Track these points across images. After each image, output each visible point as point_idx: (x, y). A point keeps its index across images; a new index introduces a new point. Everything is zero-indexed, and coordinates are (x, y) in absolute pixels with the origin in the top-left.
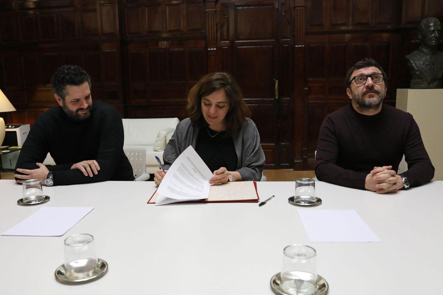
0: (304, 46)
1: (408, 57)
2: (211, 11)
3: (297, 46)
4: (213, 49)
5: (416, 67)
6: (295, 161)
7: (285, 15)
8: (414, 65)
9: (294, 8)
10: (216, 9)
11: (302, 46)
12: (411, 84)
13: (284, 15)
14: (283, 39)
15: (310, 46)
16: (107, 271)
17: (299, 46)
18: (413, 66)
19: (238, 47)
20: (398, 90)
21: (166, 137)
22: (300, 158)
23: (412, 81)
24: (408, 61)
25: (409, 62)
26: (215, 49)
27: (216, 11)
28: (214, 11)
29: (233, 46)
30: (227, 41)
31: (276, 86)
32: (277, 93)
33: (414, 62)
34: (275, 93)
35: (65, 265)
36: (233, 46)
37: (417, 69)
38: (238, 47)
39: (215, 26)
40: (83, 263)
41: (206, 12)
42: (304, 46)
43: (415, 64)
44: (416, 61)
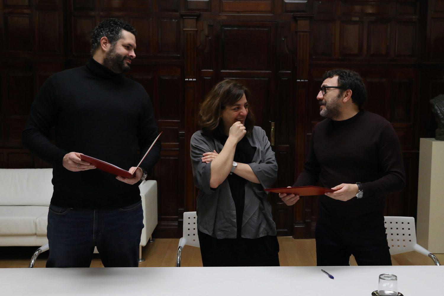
0: (307, 81)
1: (432, 101)
3: (299, 81)
4: (191, 80)
5: (441, 115)
6: (296, 226)
8: (439, 112)
9: (296, 32)
10: (196, 28)
11: (305, 81)
12: (436, 134)
18: (437, 114)
22: (301, 222)
23: (437, 130)
25: (434, 108)
27: (197, 31)
30: (210, 69)
31: (272, 129)
33: (439, 109)
34: (271, 138)
37: (442, 117)
41: (184, 31)
42: (307, 81)
43: (441, 112)
44: (441, 107)
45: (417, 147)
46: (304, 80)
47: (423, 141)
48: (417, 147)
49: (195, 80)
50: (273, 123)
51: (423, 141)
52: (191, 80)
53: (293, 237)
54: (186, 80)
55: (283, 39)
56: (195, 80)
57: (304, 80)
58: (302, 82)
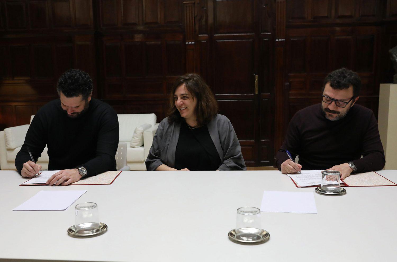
0: (284, 40)
1: (391, 51)
2: (190, 3)
3: (278, 40)
4: (191, 43)
7: (265, 8)
10: (194, 1)
11: (283, 40)
13: (264, 7)
14: (263, 32)
15: (292, 39)
16: (106, 230)
17: (280, 40)
19: (217, 41)
20: (381, 85)
21: (143, 133)
23: (395, 76)
24: (391, 55)
26: (193, 43)
27: (194, 3)
28: (192, 3)
29: (211, 39)
30: (206, 34)
31: (256, 81)
32: (257, 89)
34: (255, 88)
35: (75, 226)
36: (211, 39)
38: (217, 41)
39: (193, 19)
40: (88, 225)
41: (184, 4)
42: (284, 40)
45: (377, 92)
46: (282, 39)
47: (382, 86)
48: (377, 92)
49: (193, 43)
50: (257, 76)
51: (382, 86)
52: (191, 43)
53: (274, 167)
54: (186, 43)
55: (264, 6)
56: (193, 43)
57: (282, 39)
58: (280, 41)
